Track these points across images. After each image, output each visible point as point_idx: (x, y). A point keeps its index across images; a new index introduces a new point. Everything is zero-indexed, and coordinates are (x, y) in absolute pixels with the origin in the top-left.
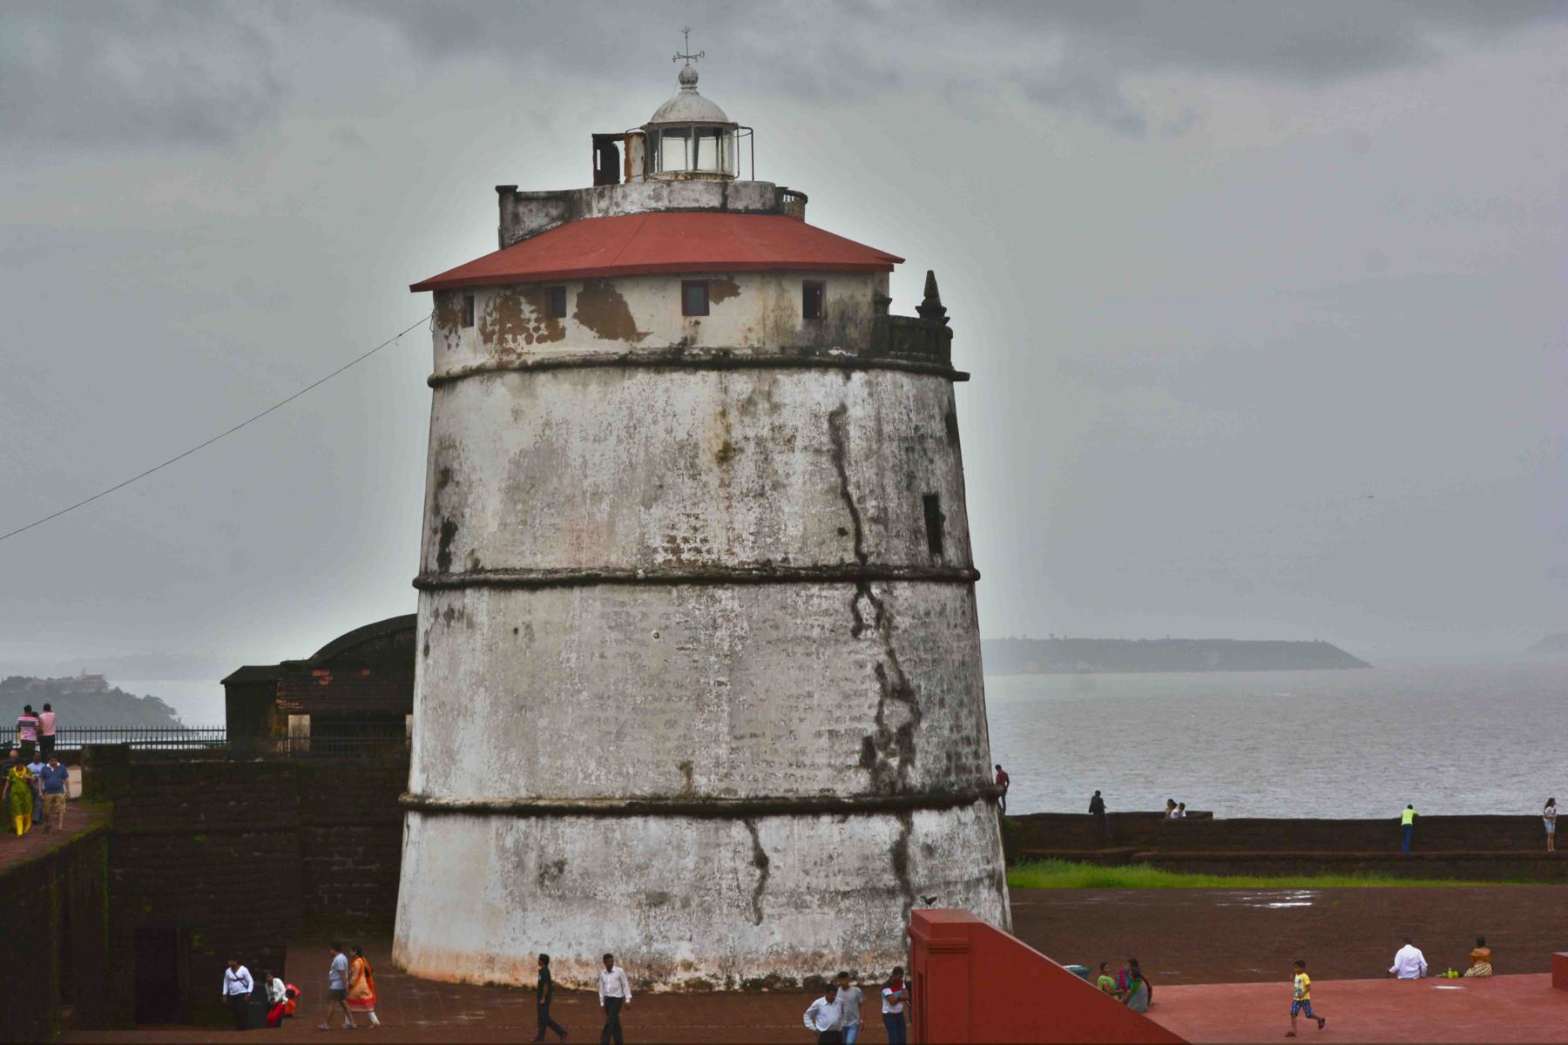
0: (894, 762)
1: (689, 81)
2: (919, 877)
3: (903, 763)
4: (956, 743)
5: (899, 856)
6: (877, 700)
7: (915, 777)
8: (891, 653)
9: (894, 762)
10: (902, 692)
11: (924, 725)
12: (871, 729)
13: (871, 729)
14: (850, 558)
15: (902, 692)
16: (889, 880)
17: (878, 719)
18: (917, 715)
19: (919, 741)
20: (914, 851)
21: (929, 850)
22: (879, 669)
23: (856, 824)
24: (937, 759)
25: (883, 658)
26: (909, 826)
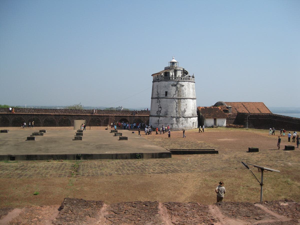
2: (160, 122)
3: (160, 113)
5: (158, 121)
7: (161, 114)
8: (160, 104)
9: (159, 113)
10: (161, 108)
12: (157, 110)
13: (157, 110)
14: (157, 97)
15: (161, 108)
16: (158, 123)
18: (162, 109)
23: (156, 117)
25: (159, 104)
26: (159, 119)
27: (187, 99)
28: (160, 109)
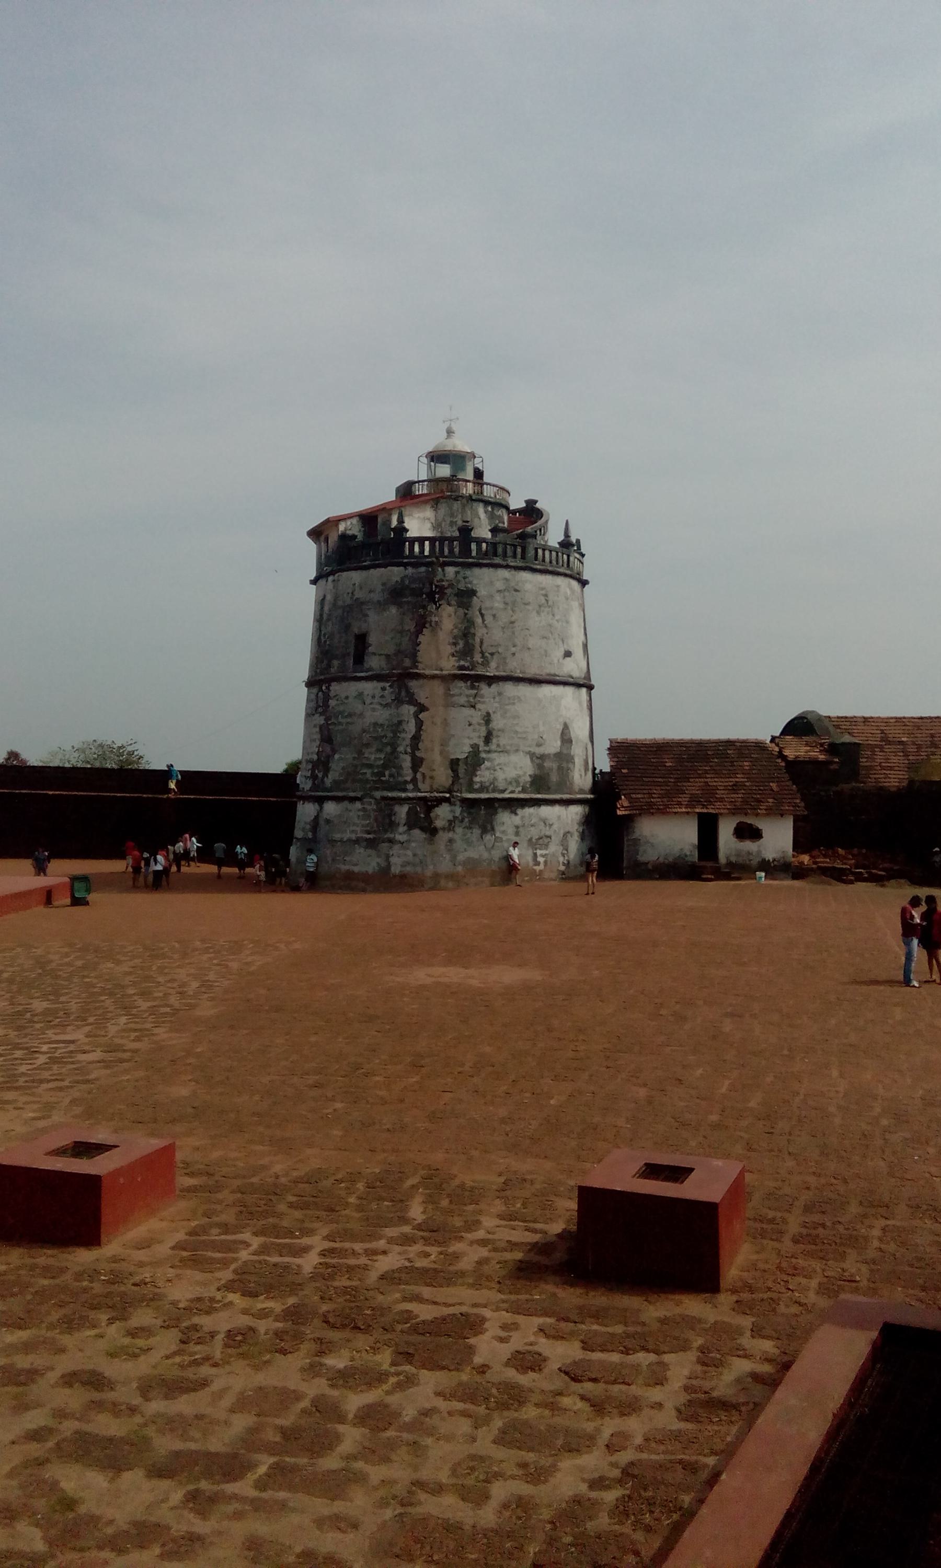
0: (320, 775)
1: (450, 432)
2: (321, 833)
3: (323, 777)
4: (356, 766)
6: (318, 743)
9: (320, 775)
11: (336, 756)
12: (315, 757)
16: (310, 835)
17: (318, 753)
18: (334, 751)
19: (333, 765)
20: (322, 822)
21: (328, 821)
22: (321, 727)
24: (341, 775)
26: (321, 808)
27: (491, 680)
28: (328, 749)
